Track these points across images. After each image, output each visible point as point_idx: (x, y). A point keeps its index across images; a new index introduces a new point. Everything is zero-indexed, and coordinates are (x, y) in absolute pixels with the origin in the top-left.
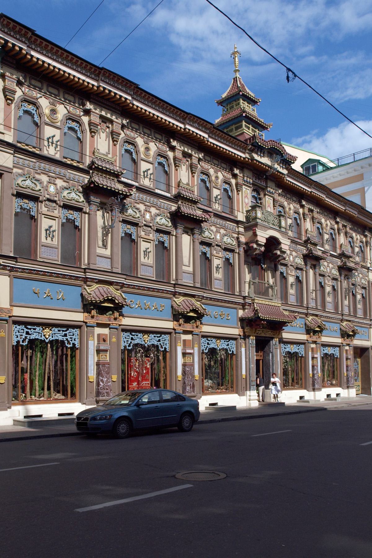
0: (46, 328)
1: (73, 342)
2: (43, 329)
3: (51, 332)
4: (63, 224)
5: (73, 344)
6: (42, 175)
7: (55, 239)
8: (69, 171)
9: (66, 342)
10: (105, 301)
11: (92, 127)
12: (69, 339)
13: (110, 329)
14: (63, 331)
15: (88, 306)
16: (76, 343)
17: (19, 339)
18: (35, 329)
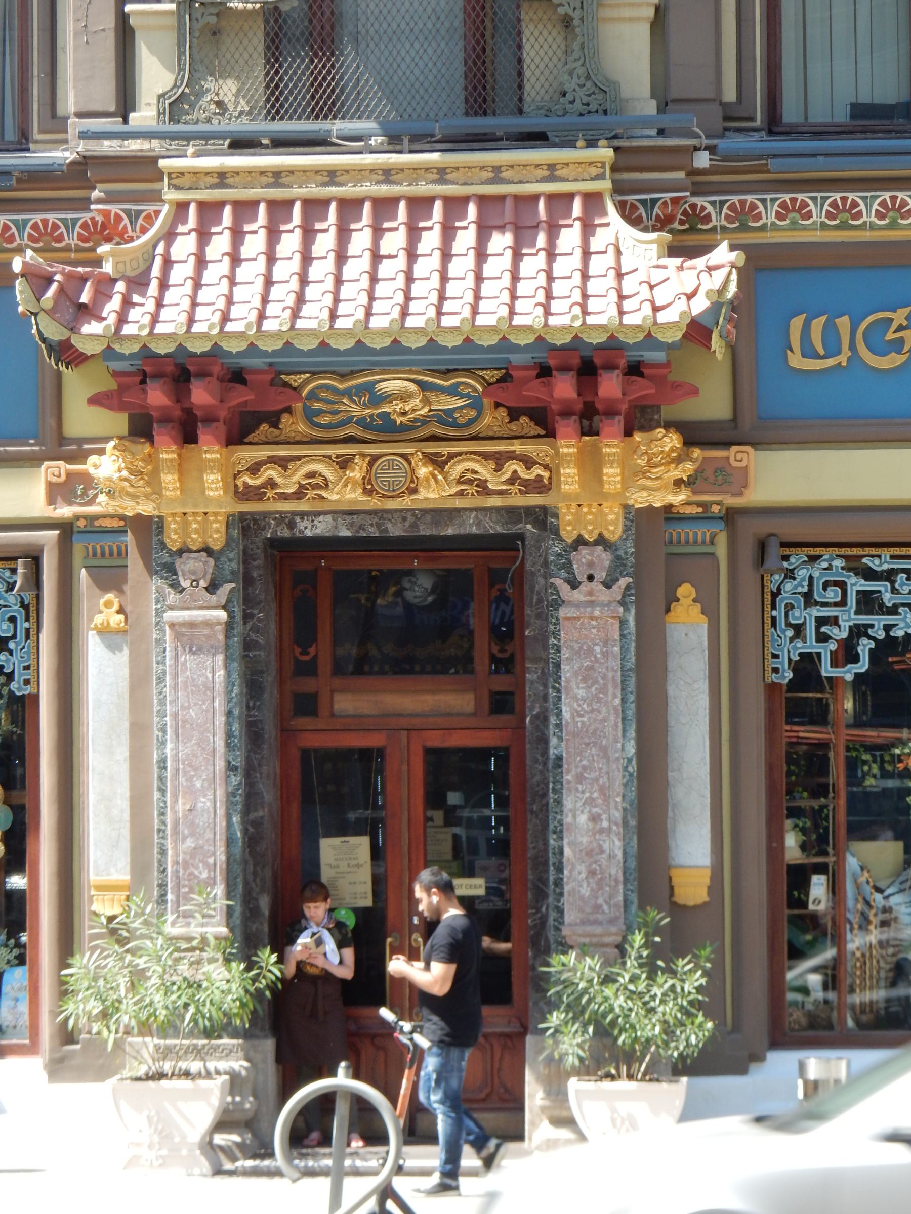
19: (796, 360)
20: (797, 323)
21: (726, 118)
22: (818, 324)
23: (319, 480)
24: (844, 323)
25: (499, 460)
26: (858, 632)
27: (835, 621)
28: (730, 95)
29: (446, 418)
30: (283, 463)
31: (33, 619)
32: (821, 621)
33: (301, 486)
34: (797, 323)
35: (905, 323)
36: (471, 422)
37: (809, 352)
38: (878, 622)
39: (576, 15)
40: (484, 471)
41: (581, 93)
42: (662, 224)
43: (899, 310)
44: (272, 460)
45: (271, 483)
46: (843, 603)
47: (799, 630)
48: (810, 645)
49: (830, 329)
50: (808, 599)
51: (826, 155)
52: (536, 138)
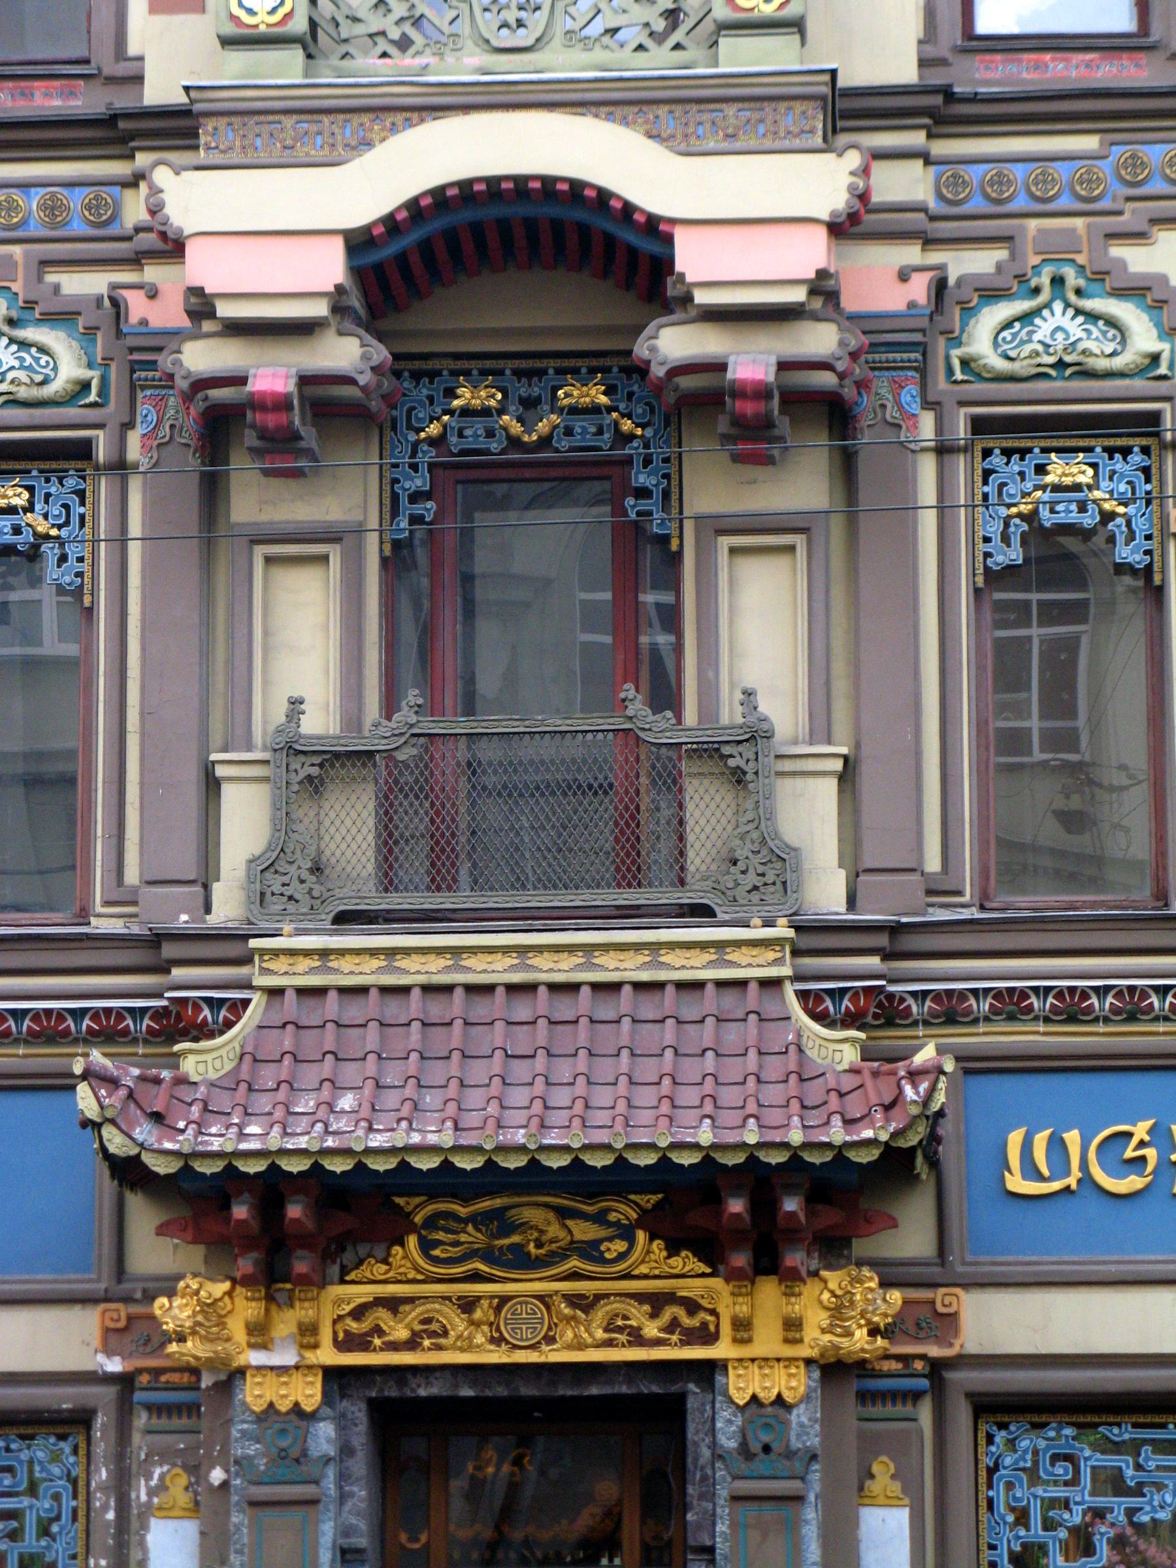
19: (1017, 1183)
20: (1015, 1139)
21: (930, 892)
22: (1041, 1140)
23: (434, 1326)
24: (1072, 1138)
25: (656, 1302)
27: (1066, 1504)
28: (933, 864)
29: (590, 1250)
30: (393, 1304)
31: (82, 1496)
32: (1052, 1503)
33: (415, 1334)
34: (1015, 1139)
35: (1147, 1138)
36: (622, 1256)
37: (1031, 1171)
38: (1119, 1506)
39: (750, 768)
40: (638, 1315)
41: (756, 860)
42: (851, 1020)
43: (1140, 1124)
44: (379, 1302)
45: (378, 1331)
46: (1074, 1482)
47: (1022, 1517)
48: (1036, 1531)
49: (1057, 1145)
50: (1033, 1475)
52: (701, 912)
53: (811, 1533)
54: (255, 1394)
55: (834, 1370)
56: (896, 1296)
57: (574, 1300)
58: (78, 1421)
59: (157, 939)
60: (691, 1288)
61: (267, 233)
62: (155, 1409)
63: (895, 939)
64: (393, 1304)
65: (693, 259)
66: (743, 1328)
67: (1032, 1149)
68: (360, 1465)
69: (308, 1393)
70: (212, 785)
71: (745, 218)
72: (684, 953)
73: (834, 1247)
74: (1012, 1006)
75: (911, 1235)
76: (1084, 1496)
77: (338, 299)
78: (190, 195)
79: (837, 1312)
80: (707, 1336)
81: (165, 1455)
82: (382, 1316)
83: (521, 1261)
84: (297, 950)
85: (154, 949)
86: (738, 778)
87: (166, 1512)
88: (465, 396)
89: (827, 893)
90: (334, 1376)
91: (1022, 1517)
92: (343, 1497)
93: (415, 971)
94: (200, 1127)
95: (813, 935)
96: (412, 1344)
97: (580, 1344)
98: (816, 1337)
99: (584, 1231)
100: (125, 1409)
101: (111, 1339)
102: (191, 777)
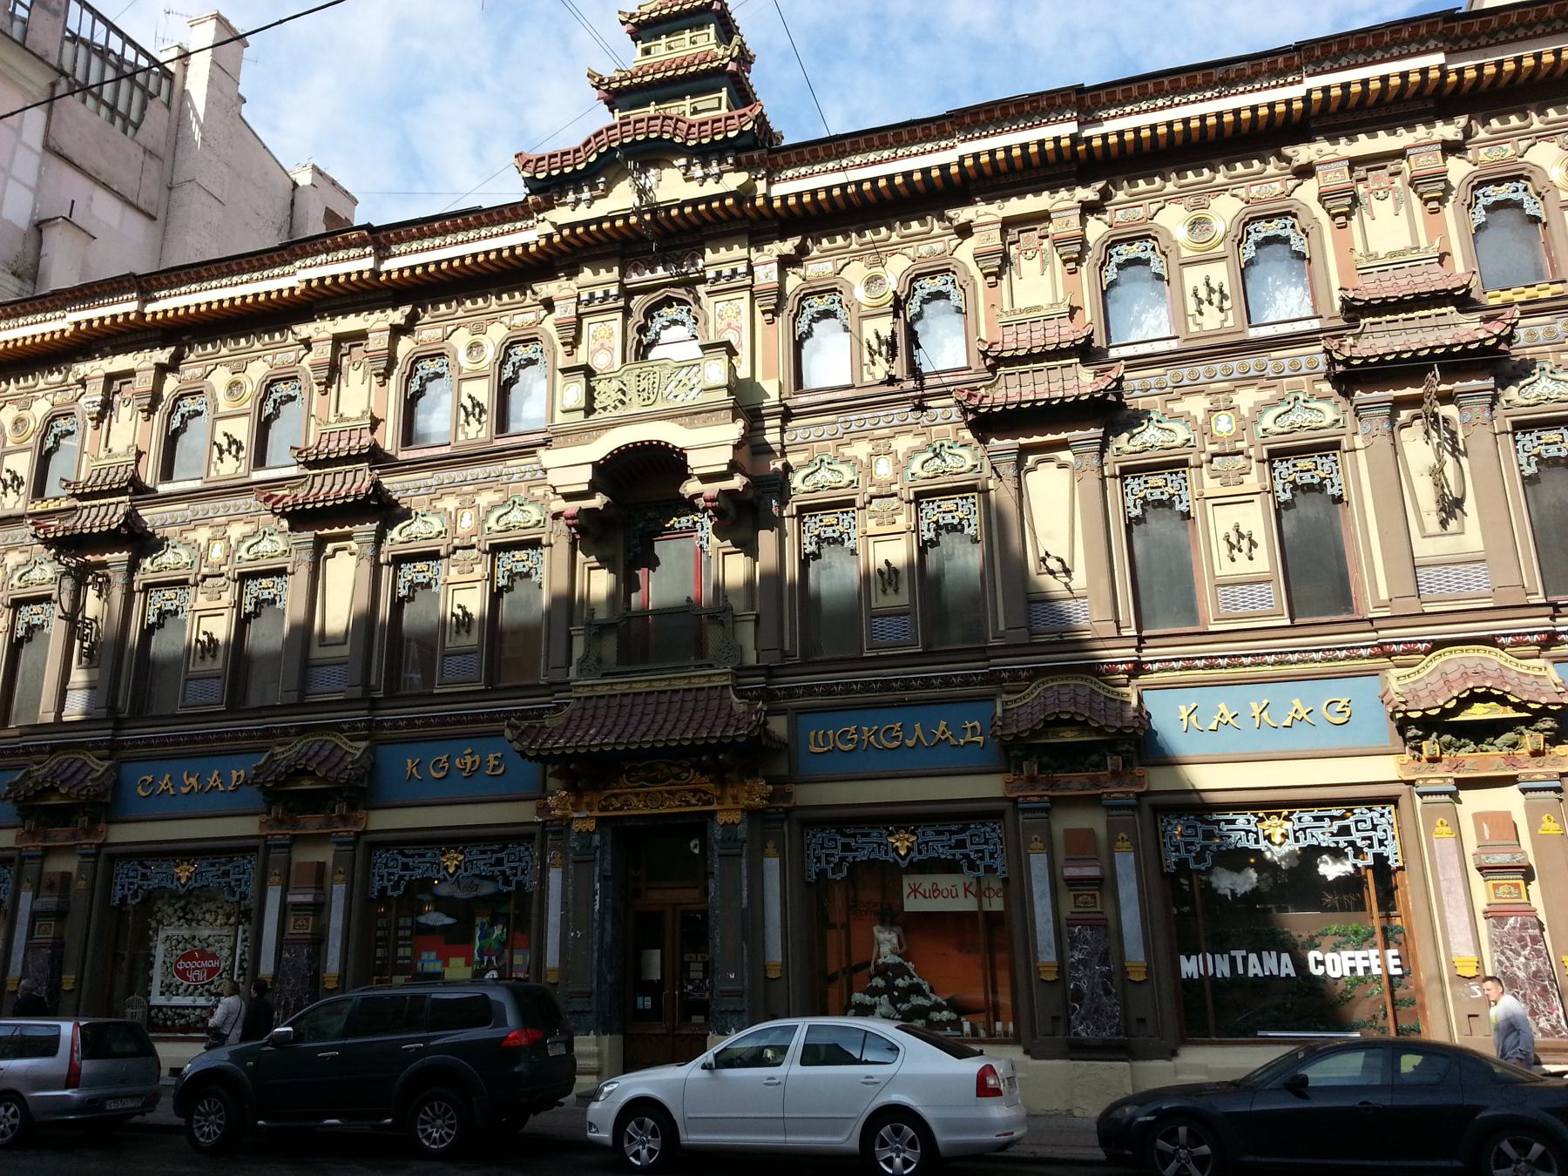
0: (1268, 815)
1: (1377, 849)
2: (1261, 820)
3: (1288, 825)
4: (1281, 509)
5: (1377, 856)
6: (1188, 400)
7: (1261, 553)
8: (1274, 355)
9: (1349, 850)
10: (1464, 703)
11: (1328, 204)
12: (1360, 843)
13: (1524, 791)
14: (1333, 818)
15: (1423, 728)
16: (1387, 852)
17: (1183, 854)
18: (1233, 822)
19: (814, 749)
25: (695, 792)
26: (842, 859)
30: (616, 796)
37: (817, 744)
38: (850, 856)
40: (689, 796)
47: (819, 860)
51: (274, 707)
52: (711, 666)
53: (744, 866)
54: (576, 827)
55: (751, 813)
56: (770, 788)
57: (669, 792)
58: (529, 838)
59: (551, 684)
60: (704, 787)
61: (571, 466)
62: (554, 833)
63: (769, 672)
64: (616, 796)
65: (694, 461)
66: (721, 800)
67: (820, 738)
68: (608, 849)
69: (591, 826)
70: (570, 638)
71: (709, 447)
72: (699, 679)
73: (752, 773)
74: (809, 691)
75: (782, 769)
76: (838, 853)
77: (591, 483)
78: (546, 457)
79: (750, 793)
80: (711, 803)
81: (554, 848)
82: (613, 800)
83: (656, 781)
84: (584, 685)
85: (552, 687)
86: (722, 624)
87: (554, 866)
88: (651, 514)
89: (751, 658)
90: (598, 819)
91: (819, 860)
92: (602, 859)
93: (619, 689)
94: (545, 741)
95: (741, 671)
96: (621, 809)
97: (670, 807)
98: (744, 802)
99: (675, 770)
100: (544, 834)
101: (539, 811)
102: (564, 636)
